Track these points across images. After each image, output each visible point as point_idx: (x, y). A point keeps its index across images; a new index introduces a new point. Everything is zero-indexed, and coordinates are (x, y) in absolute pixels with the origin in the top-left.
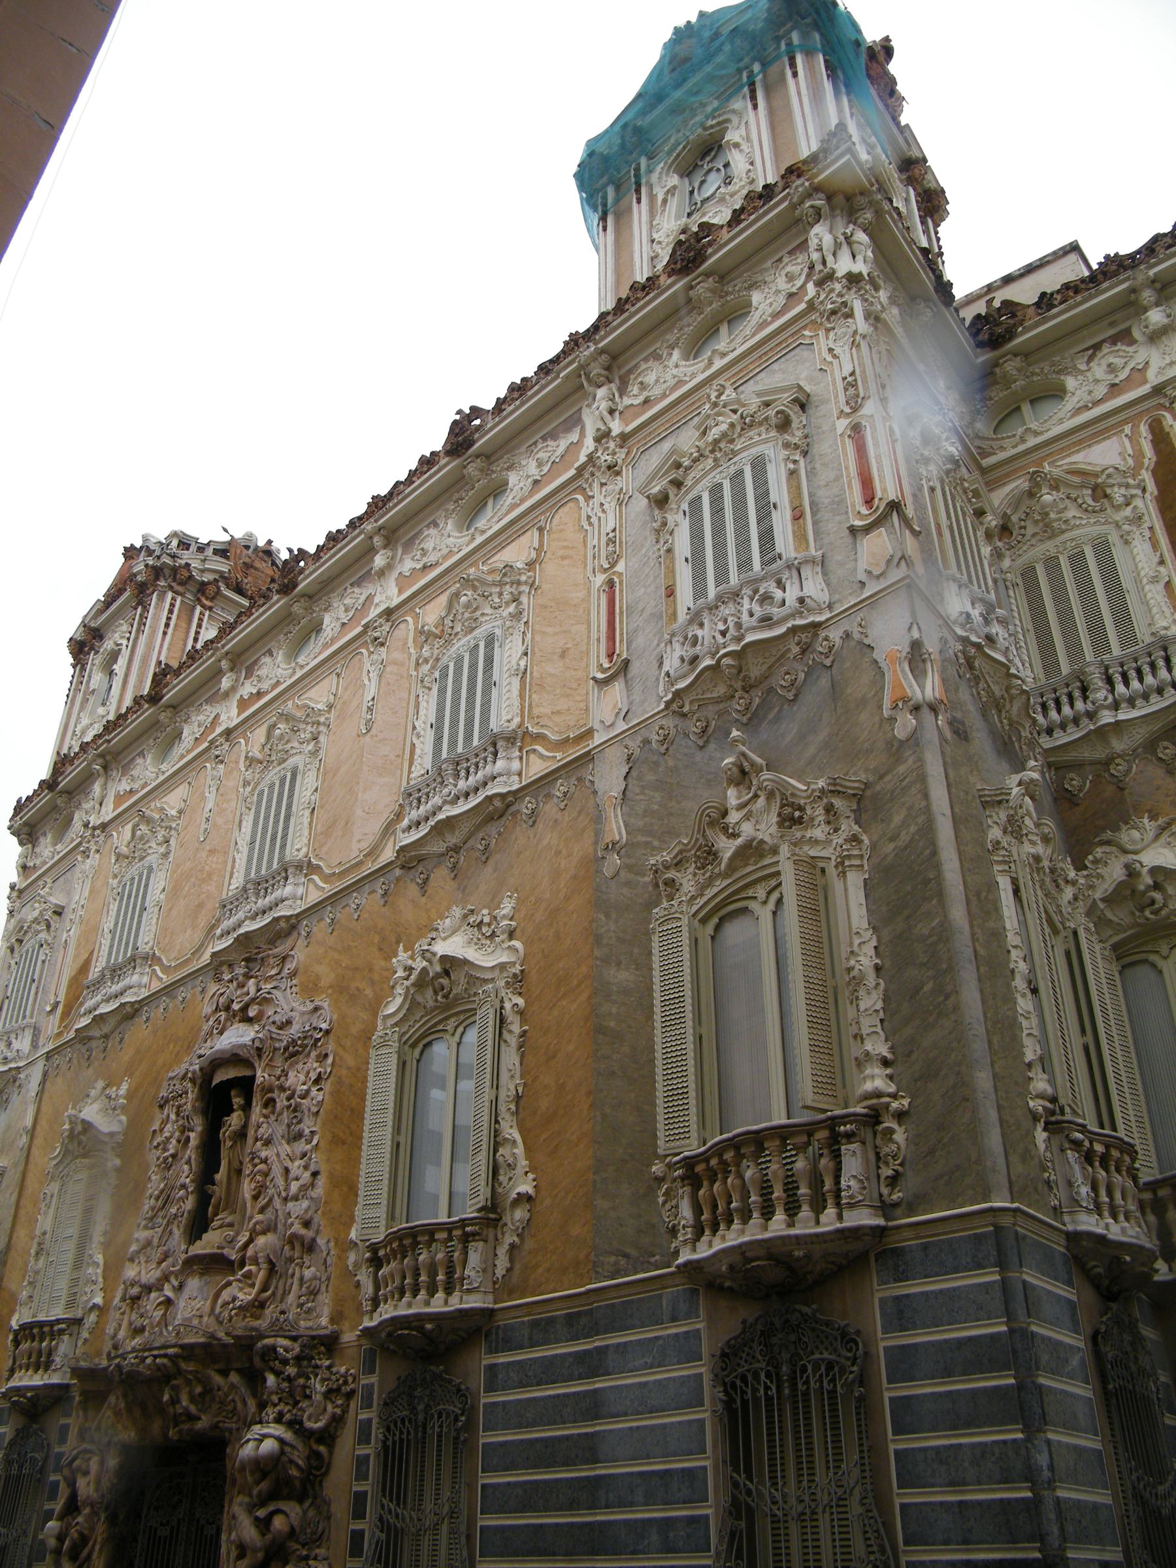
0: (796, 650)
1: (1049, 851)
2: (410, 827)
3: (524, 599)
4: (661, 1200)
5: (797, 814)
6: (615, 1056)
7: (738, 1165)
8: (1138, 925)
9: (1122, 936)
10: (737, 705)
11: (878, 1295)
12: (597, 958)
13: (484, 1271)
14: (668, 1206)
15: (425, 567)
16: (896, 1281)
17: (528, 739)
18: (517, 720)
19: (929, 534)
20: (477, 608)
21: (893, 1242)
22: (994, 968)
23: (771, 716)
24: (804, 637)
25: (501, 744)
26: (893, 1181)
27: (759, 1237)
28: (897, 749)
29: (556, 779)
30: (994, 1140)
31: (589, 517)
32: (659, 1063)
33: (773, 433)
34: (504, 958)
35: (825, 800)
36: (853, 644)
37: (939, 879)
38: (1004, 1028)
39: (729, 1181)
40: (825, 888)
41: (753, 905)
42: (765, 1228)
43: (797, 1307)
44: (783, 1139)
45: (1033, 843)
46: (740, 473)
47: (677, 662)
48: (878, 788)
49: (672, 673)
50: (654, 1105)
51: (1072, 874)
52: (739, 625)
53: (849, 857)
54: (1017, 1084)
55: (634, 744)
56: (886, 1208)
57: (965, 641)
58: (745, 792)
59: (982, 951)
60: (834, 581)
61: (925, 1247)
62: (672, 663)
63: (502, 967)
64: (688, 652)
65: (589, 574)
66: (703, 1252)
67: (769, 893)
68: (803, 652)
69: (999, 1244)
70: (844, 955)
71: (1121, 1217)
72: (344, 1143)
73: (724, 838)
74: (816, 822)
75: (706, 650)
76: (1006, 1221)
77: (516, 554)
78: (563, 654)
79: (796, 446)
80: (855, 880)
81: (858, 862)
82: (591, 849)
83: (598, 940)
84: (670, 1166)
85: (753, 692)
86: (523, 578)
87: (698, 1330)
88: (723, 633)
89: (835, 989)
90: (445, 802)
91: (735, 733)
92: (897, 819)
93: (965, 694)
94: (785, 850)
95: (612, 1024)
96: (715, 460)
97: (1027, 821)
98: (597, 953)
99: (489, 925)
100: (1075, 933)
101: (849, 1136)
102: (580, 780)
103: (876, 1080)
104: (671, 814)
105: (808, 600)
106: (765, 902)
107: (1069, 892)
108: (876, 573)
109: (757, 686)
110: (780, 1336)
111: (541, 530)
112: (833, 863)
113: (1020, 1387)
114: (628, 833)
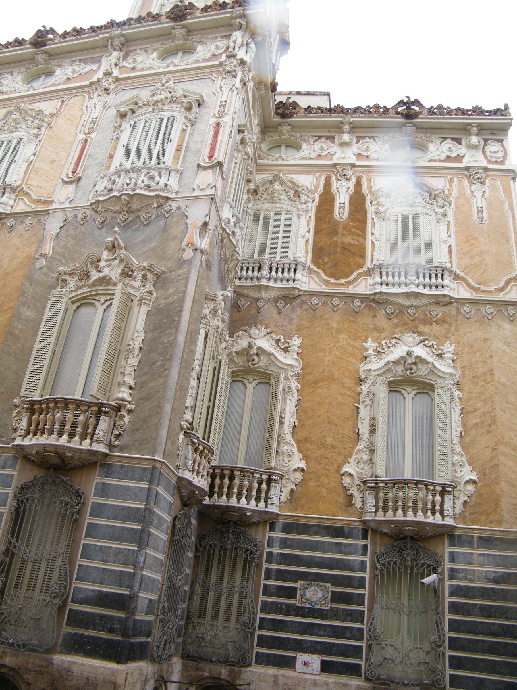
0: (156, 205)
1: (223, 326)
3: (43, 129)
4: (14, 415)
5: (130, 273)
6: (13, 347)
7: (54, 410)
8: (245, 367)
9: (237, 369)
10: (122, 217)
11: (96, 481)
12: (19, 301)
14: (16, 418)
16: (105, 477)
17: (22, 193)
18: (19, 182)
19: (227, 181)
20: (19, 123)
21: (109, 461)
22: (187, 365)
23: (134, 228)
24: (161, 201)
25: (8, 190)
26: (118, 436)
27: (54, 443)
28: (182, 263)
29: (29, 216)
30: (164, 433)
31: (87, 107)
32: (33, 356)
33: (183, 110)
35: (144, 272)
36: (180, 212)
37: (179, 322)
38: (182, 390)
39: (48, 416)
40: (130, 308)
41: (97, 303)
42: (58, 440)
43: (61, 476)
44: (78, 406)
45: (218, 320)
46: (162, 120)
47: (102, 188)
48: (168, 275)
49: (99, 191)
50: (25, 374)
51: (227, 338)
52: (136, 184)
53: (145, 299)
54: (180, 413)
55: (70, 215)
56: (111, 446)
57: (224, 230)
58: (111, 255)
59: (185, 357)
60: (183, 183)
61: (122, 467)
62: (100, 187)
64: (110, 186)
65: (78, 132)
67: (106, 301)
68: (158, 207)
69: (152, 474)
70: (128, 338)
71: (200, 476)
73: (95, 271)
74: (137, 279)
75: (117, 188)
76: (158, 466)
77: (47, 107)
78: (52, 162)
79: (190, 120)
80: (144, 309)
81: (148, 302)
82: (33, 253)
83: (23, 294)
84: (23, 402)
85: (130, 215)
86: (46, 120)
87: (13, 475)
88: (128, 185)
89: (120, 350)
91: (116, 229)
92: (171, 291)
93: (216, 252)
94: (120, 286)
95: (17, 332)
96: (153, 109)
97: (220, 311)
98: (20, 299)
100: (220, 362)
101: (106, 413)
102: (39, 220)
103: (124, 394)
104: (76, 252)
105: (168, 186)
106: (102, 304)
107: (224, 345)
108: (201, 187)
109: (132, 212)
110: (49, 486)
111: (63, 102)
112: (138, 299)
113: (142, 531)
114: (53, 252)
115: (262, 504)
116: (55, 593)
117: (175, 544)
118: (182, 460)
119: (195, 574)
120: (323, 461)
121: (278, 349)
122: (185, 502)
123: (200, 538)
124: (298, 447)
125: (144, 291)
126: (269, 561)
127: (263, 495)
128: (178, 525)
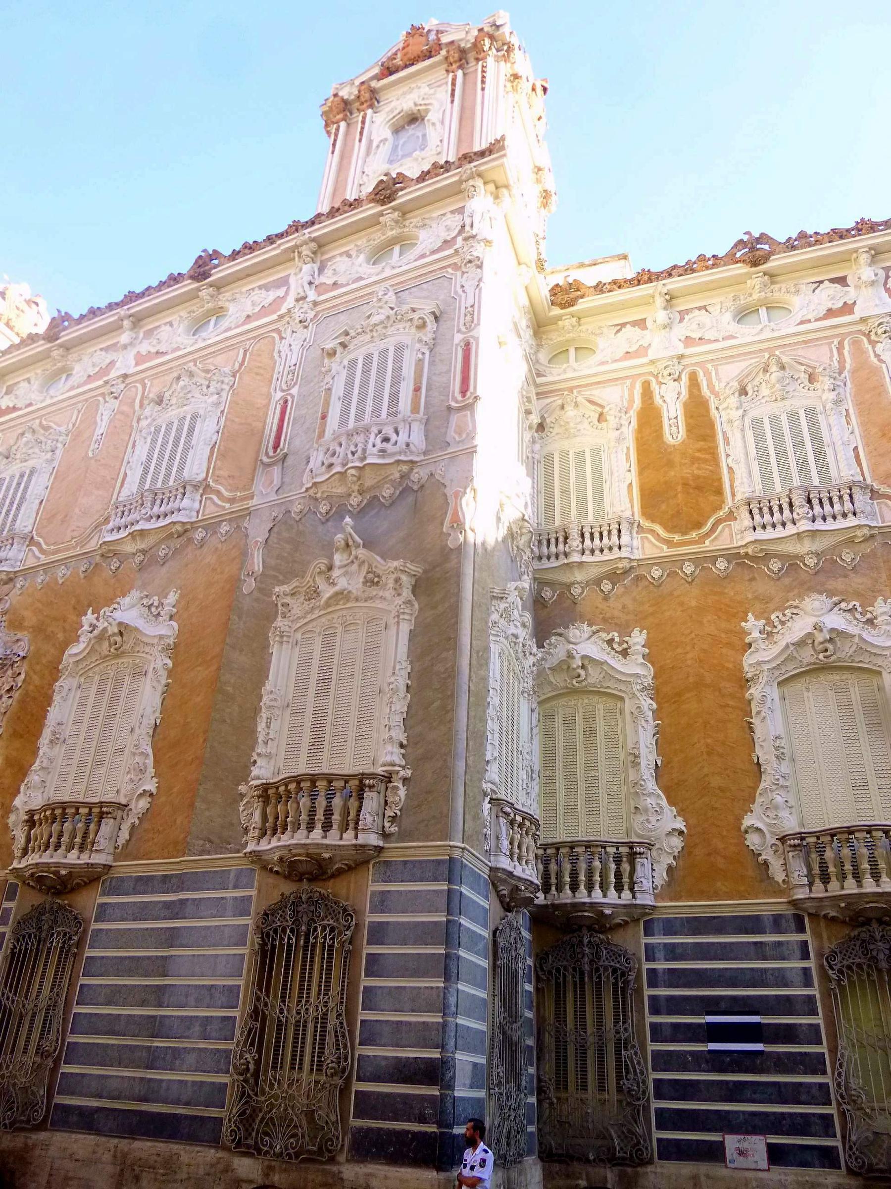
2: (113, 530)
4: (241, 809)
13: (110, 839)
14: (245, 813)
15: (157, 353)
24: (405, 468)
25: (188, 488)
26: (393, 819)
33: (413, 330)
34: (163, 632)
45: (516, 627)
51: (535, 650)
56: (385, 836)
59: (472, 687)
63: (161, 637)
65: (272, 390)
66: (264, 846)
72: (21, 736)
76: (457, 854)
90: (142, 518)
99: (157, 607)
104: (295, 561)
113: (447, 956)
115: (626, 895)
116: (332, 1068)
117: (501, 971)
118: (492, 842)
119: (540, 1019)
120: (710, 814)
121: (613, 653)
122: (508, 904)
123: (541, 958)
124: (668, 798)
125: (400, 602)
126: (652, 984)
127: (626, 880)
128: (502, 942)
